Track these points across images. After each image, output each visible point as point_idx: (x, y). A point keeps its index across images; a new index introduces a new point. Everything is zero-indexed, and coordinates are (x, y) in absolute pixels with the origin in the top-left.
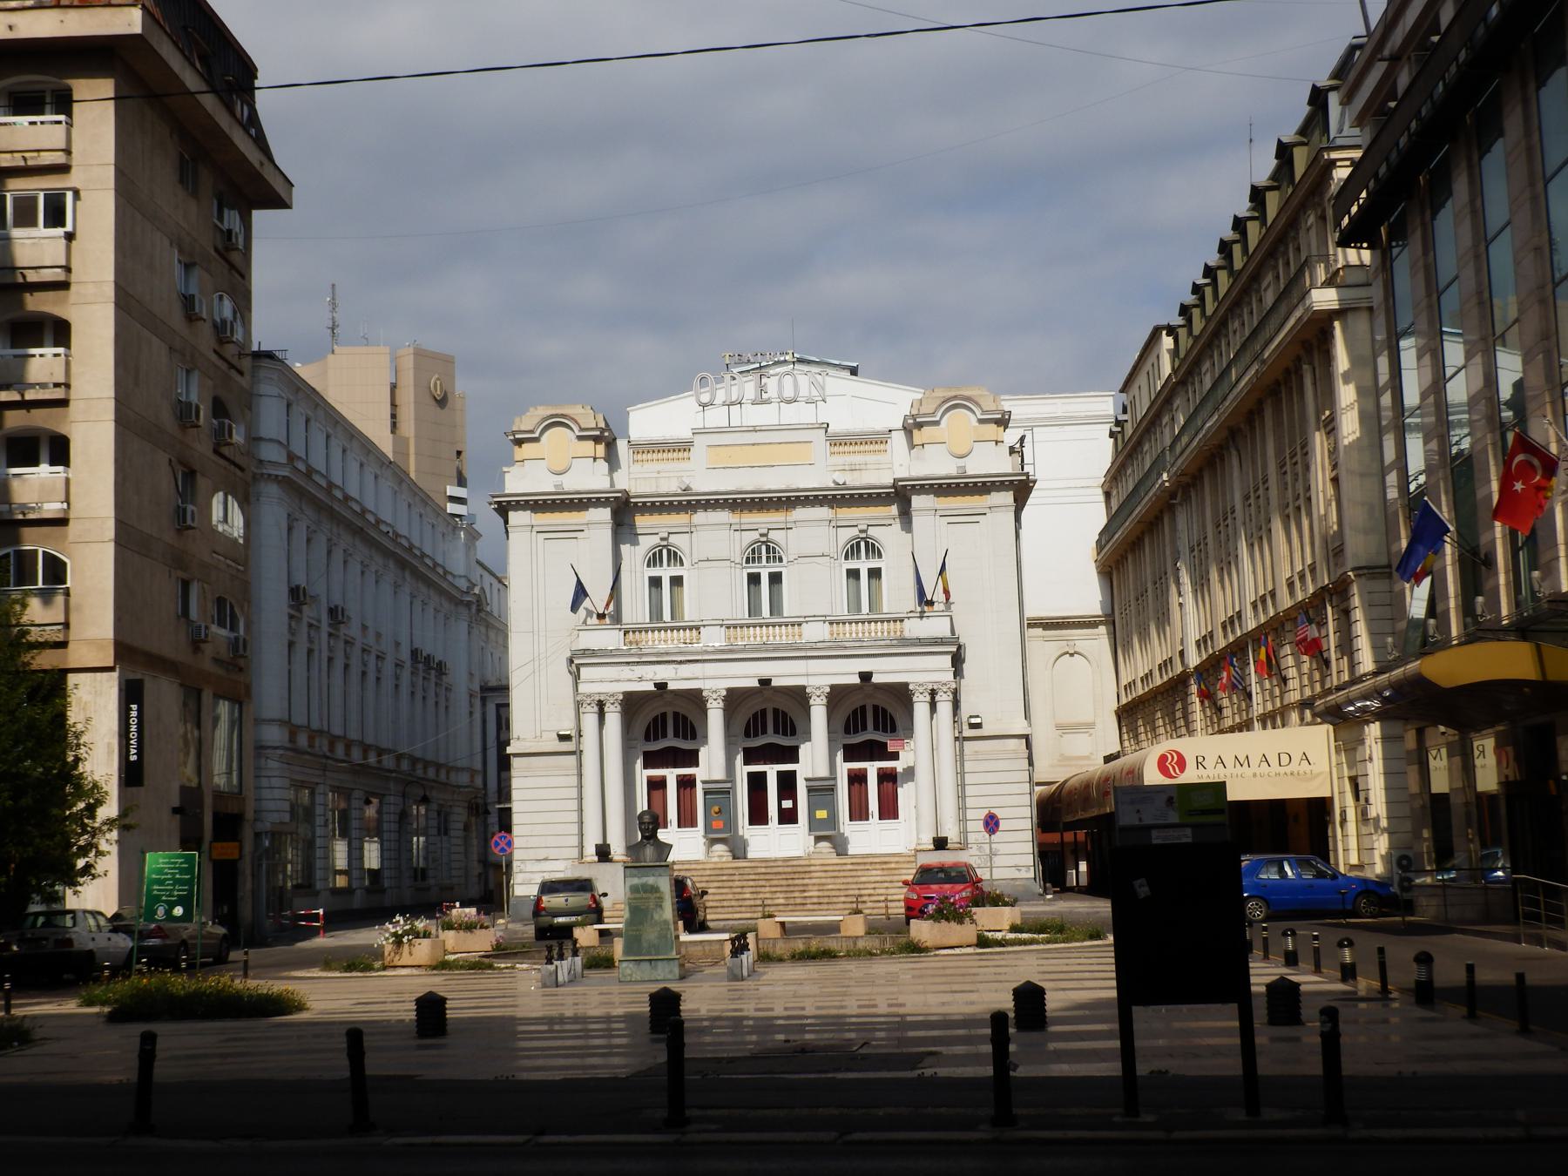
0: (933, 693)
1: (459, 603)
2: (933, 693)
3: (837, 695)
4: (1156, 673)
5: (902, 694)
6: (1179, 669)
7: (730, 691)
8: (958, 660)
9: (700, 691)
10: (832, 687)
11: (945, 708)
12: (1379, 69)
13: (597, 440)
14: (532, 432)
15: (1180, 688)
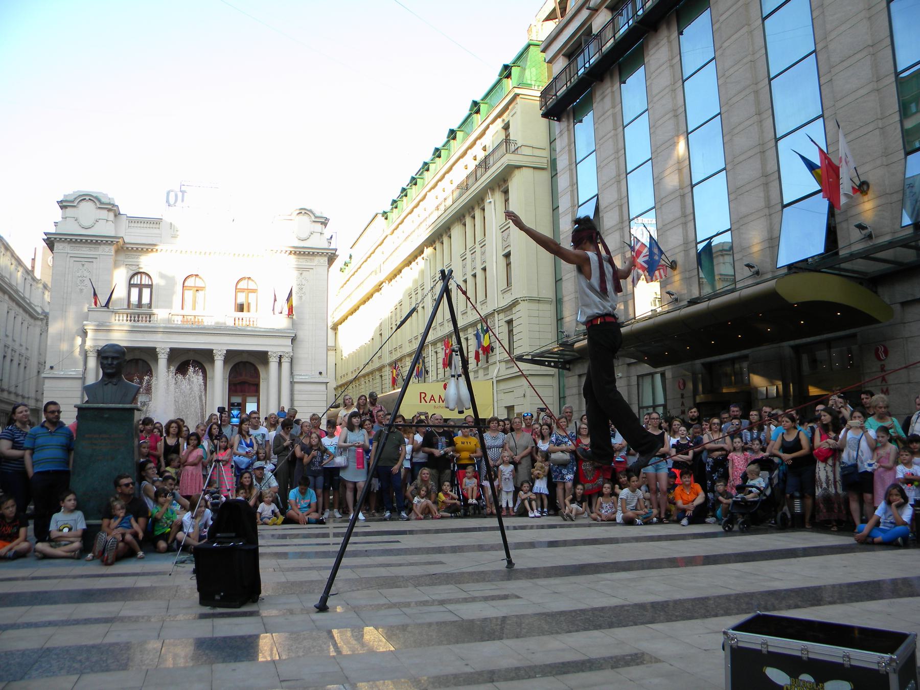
0: (280, 357)
1: (36, 319)
2: (280, 357)
3: (230, 355)
4: (350, 374)
5: (263, 357)
6: (376, 364)
7: (172, 350)
8: (294, 340)
9: (155, 348)
10: (227, 351)
11: (286, 366)
12: (585, 13)
13: (109, 210)
14: (73, 202)
15: (377, 374)
